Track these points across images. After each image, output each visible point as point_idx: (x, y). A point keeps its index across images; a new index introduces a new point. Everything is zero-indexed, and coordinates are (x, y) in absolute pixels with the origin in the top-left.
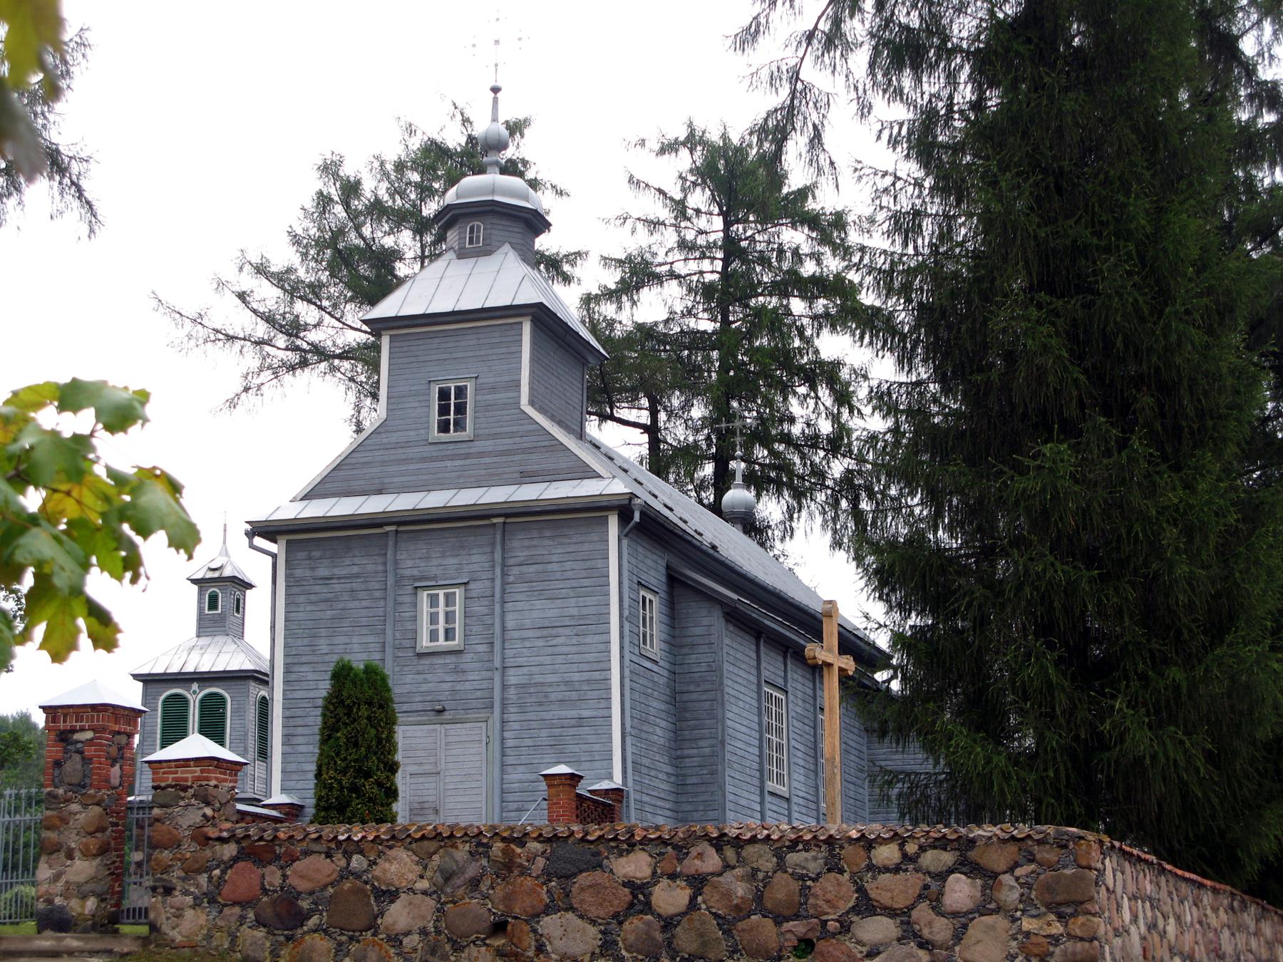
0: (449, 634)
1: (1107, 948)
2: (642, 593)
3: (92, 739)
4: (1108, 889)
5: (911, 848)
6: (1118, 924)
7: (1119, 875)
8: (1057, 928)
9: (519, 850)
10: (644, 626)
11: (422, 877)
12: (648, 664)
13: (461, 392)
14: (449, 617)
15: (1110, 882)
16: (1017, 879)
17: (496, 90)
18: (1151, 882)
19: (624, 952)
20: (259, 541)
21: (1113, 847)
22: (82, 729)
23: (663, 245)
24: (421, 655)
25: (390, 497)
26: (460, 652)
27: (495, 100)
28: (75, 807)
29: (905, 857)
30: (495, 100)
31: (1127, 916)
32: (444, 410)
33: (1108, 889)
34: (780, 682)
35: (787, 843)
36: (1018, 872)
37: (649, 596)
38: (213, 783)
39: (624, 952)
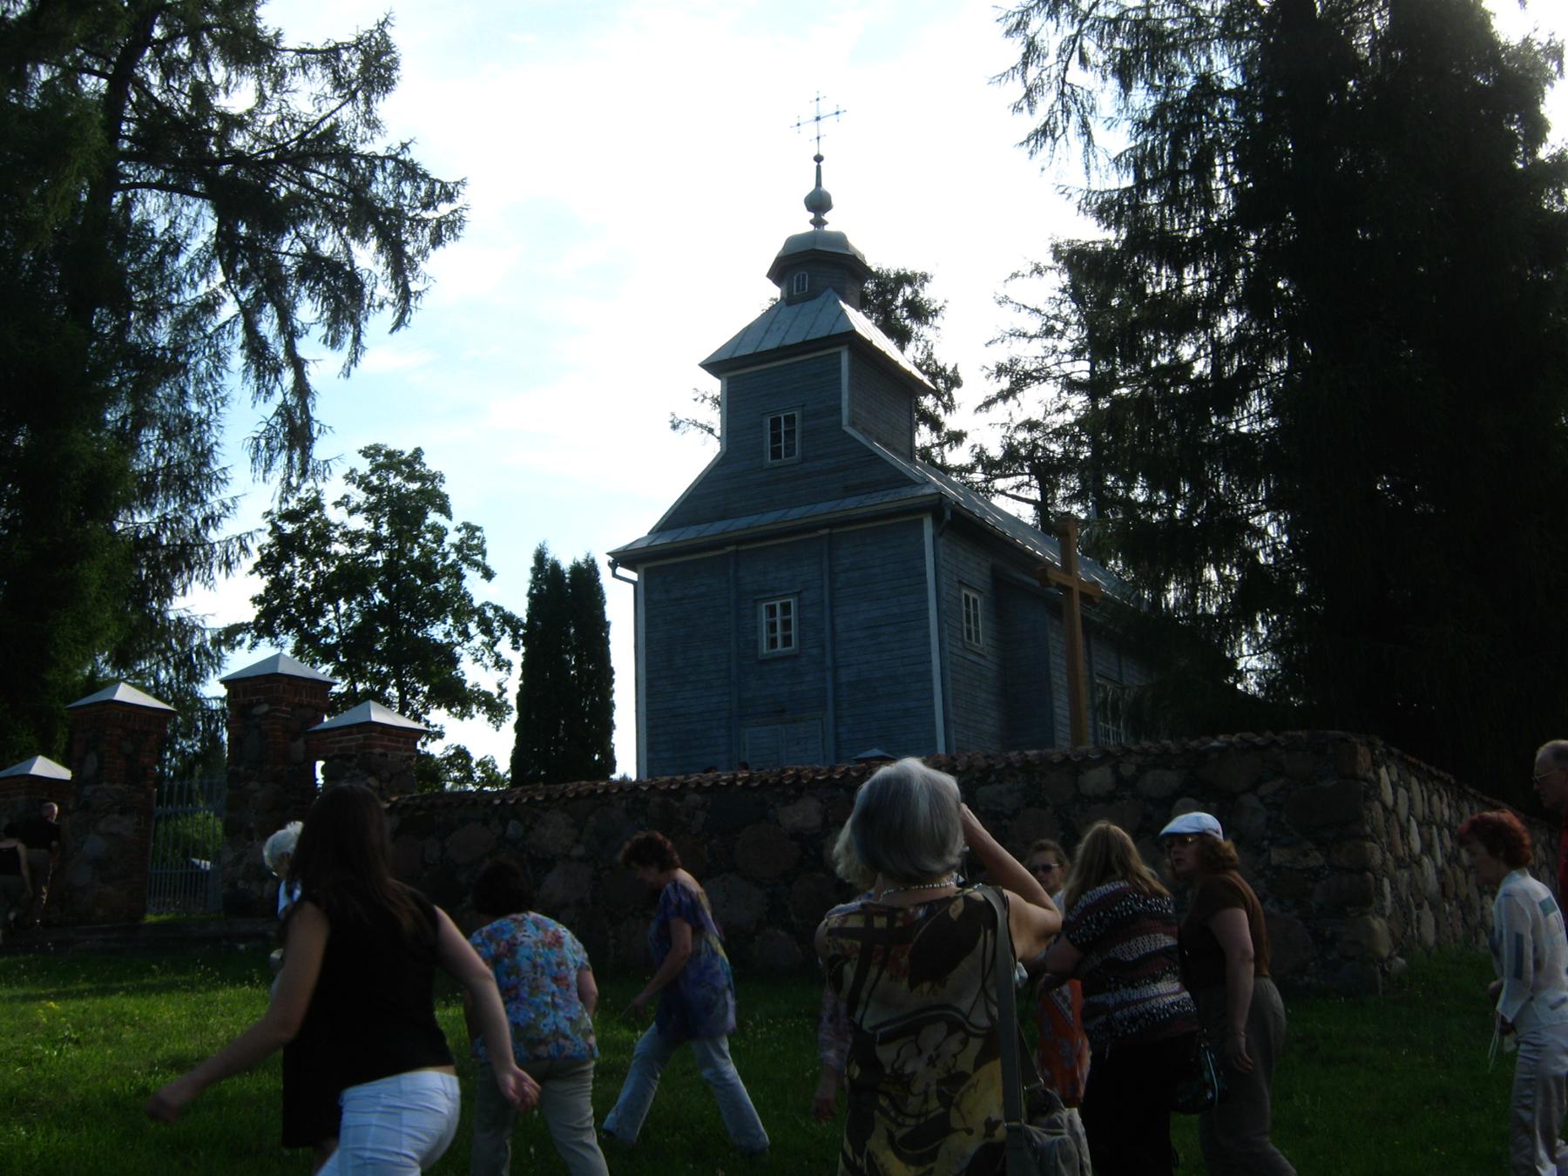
0: (787, 641)
1: (1386, 882)
2: (964, 591)
3: (266, 713)
4: (1385, 808)
5: (1128, 769)
6: (1401, 851)
7: (1402, 791)
8: (1316, 859)
9: (677, 804)
10: (968, 621)
11: (578, 841)
12: (972, 657)
13: (790, 420)
14: (786, 625)
15: (1389, 798)
16: (1262, 799)
17: (818, 159)
18: (1449, 806)
19: (793, 918)
20: (621, 571)
21: (1390, 754)
22: (259, 703)
23: (1030, 353)
24: (763, 662)
25: (729, 522)
26: (796, 656)
27: (818, 168)
28: (253, 785)
29: (1120, 781)
30: (818, 168)
31: (1416, 844)
32: (776, 438)
33: (1385, 808)
34: (1115, 676)
35: (977, 775)
36: (1265, 789)
37: (972, 595)
38: (378, 750)
39: (793, 918)
